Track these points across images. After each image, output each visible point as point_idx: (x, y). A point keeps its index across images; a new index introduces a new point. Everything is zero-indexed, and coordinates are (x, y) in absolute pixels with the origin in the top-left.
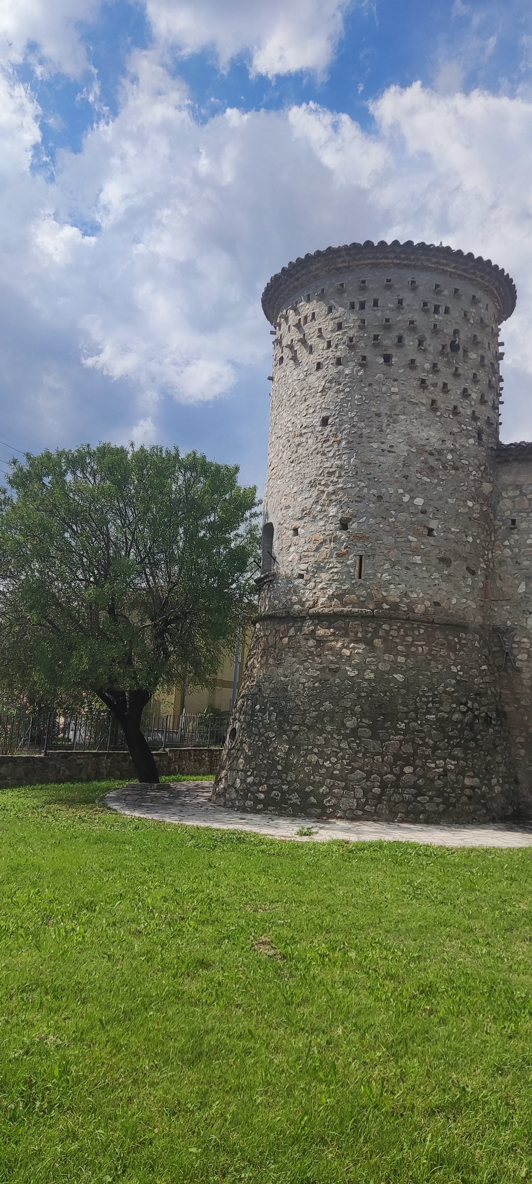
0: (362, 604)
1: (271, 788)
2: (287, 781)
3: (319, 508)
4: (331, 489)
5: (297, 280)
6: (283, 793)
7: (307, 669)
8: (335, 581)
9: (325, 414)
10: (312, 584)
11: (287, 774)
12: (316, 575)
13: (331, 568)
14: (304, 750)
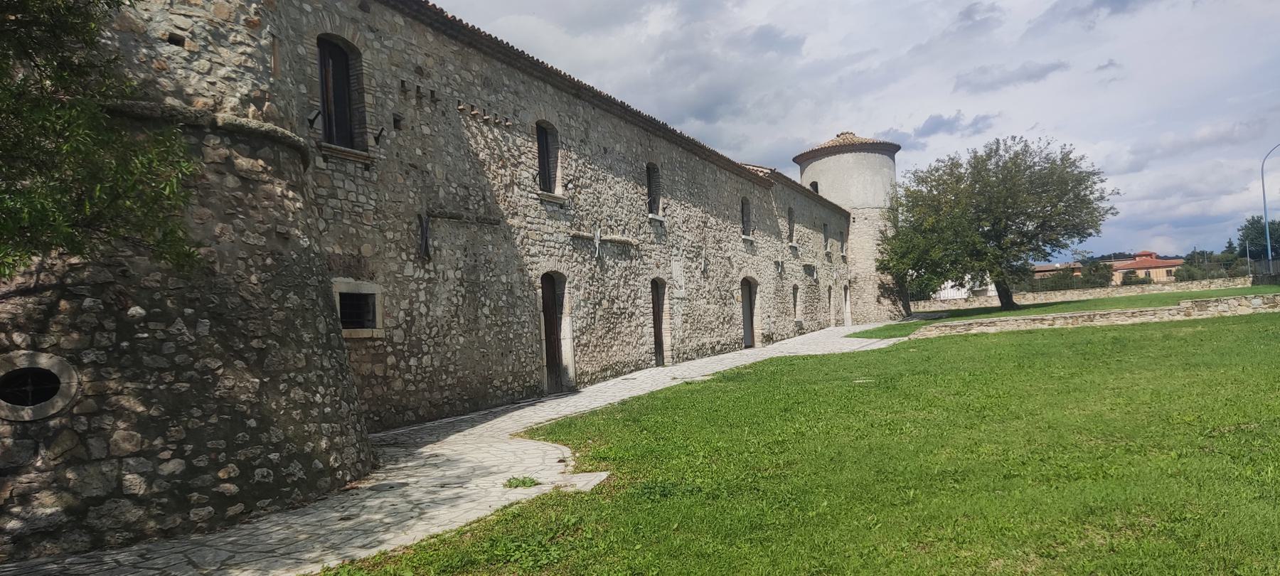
1: (246, 468)
2: (273, 445)
6: (274, 466)
7: (242, 232)
8: (249, 69)
10: (203, 64)
11: (268, 432)
12: (211, 48)
13: (241, 43)
14: (284, 381)
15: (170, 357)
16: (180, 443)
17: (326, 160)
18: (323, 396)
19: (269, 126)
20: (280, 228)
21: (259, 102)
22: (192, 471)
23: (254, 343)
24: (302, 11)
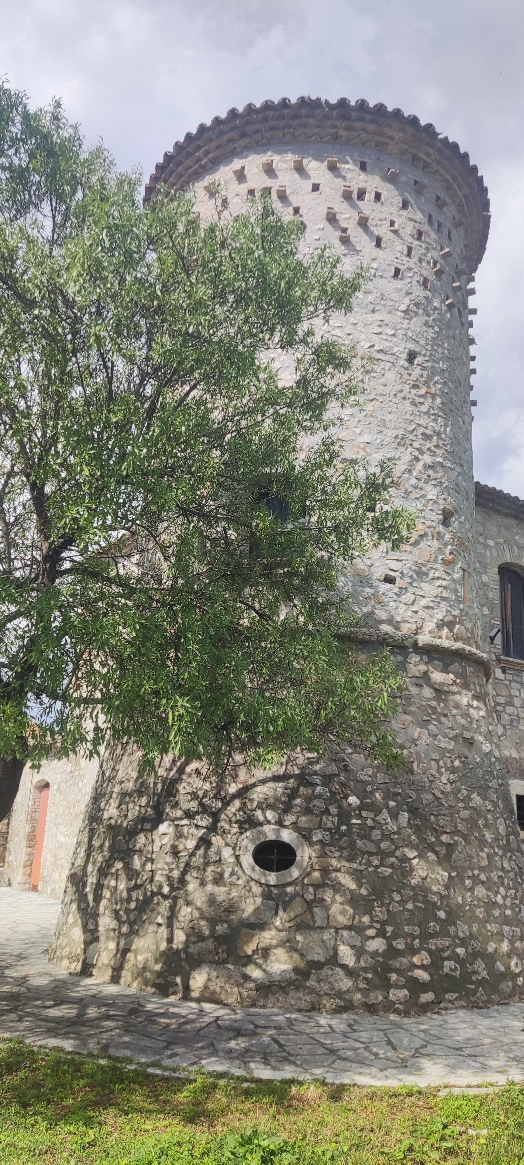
0: (467, 641)
1: (437, 957)
2: (460, 939)
3: (413, 481)
4: (427, 459)
5: (347, 129)
7: (435, 736)
8: (443, 599)
9: (411, 346)
10: (408, 597)
11: (455, 925)
12: (415, 584)
13: (438, 578)
14: (469, 878)
15: (377, 843)
16: (383, 923)
17: (504, 671)
18: (504, 898)
19: (459, 645)
20: (466, 735)
21: (450, 625)
22: (392, 952)
23: (444, 838)
24: (486, 546)
